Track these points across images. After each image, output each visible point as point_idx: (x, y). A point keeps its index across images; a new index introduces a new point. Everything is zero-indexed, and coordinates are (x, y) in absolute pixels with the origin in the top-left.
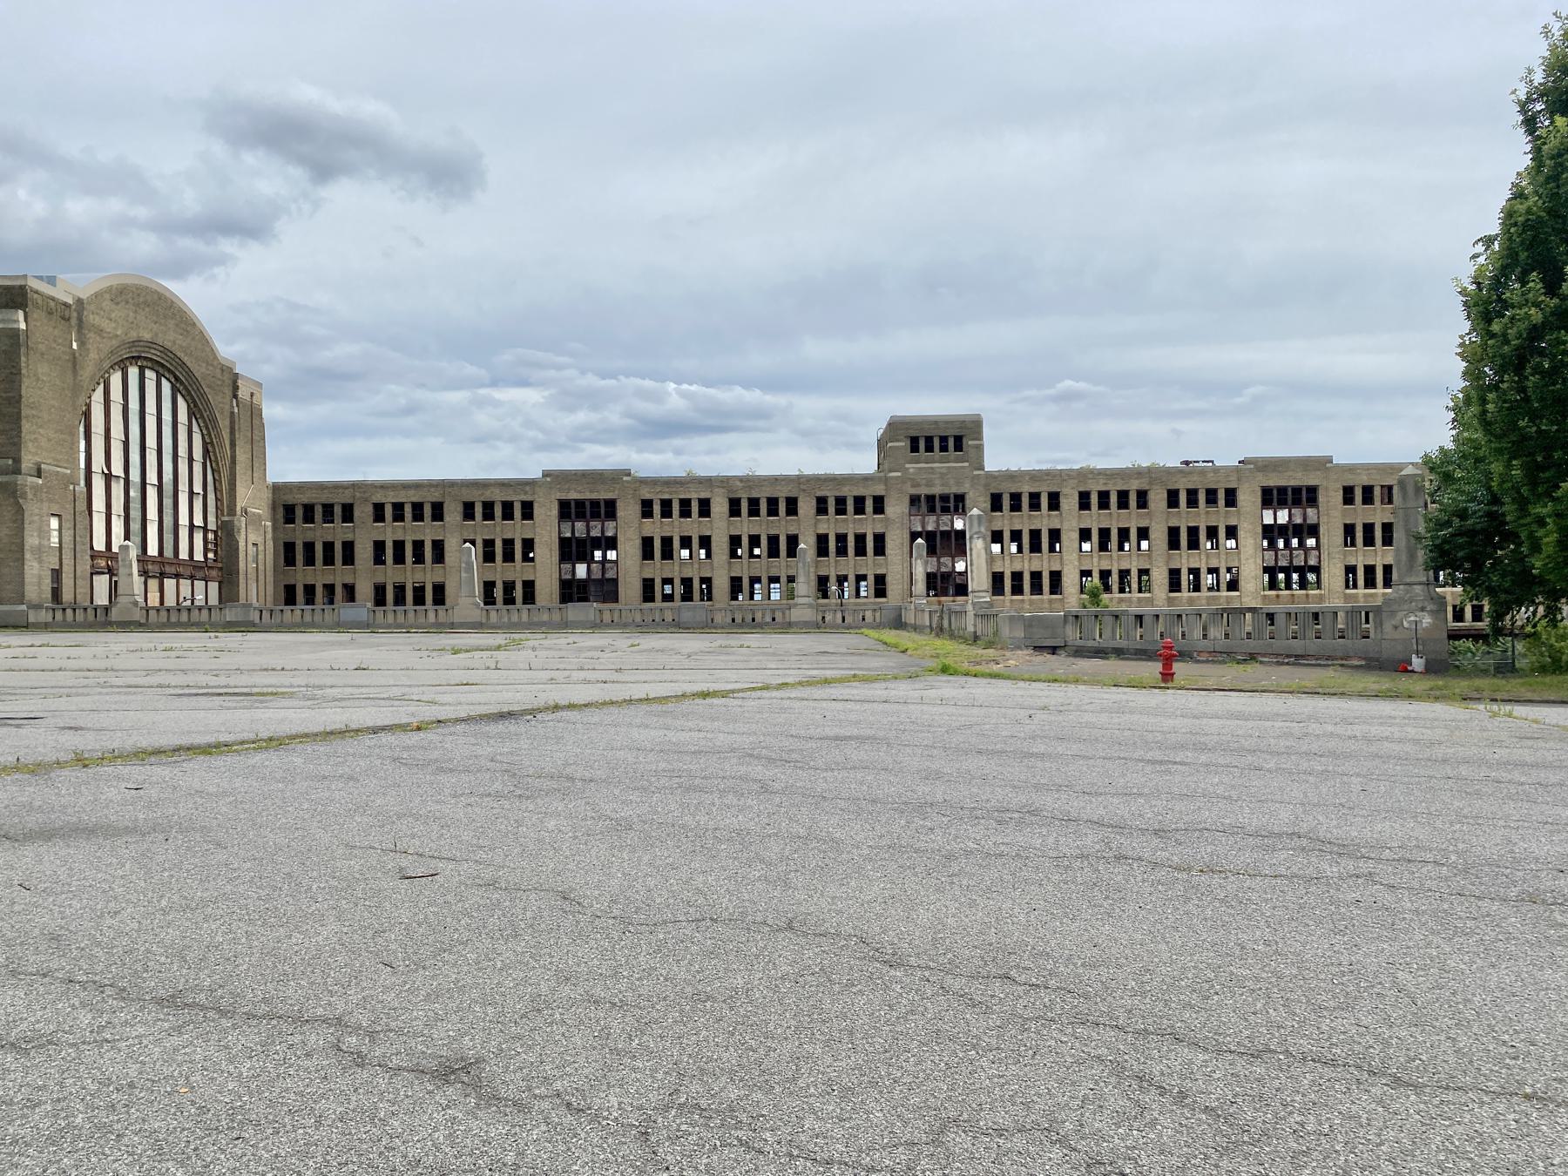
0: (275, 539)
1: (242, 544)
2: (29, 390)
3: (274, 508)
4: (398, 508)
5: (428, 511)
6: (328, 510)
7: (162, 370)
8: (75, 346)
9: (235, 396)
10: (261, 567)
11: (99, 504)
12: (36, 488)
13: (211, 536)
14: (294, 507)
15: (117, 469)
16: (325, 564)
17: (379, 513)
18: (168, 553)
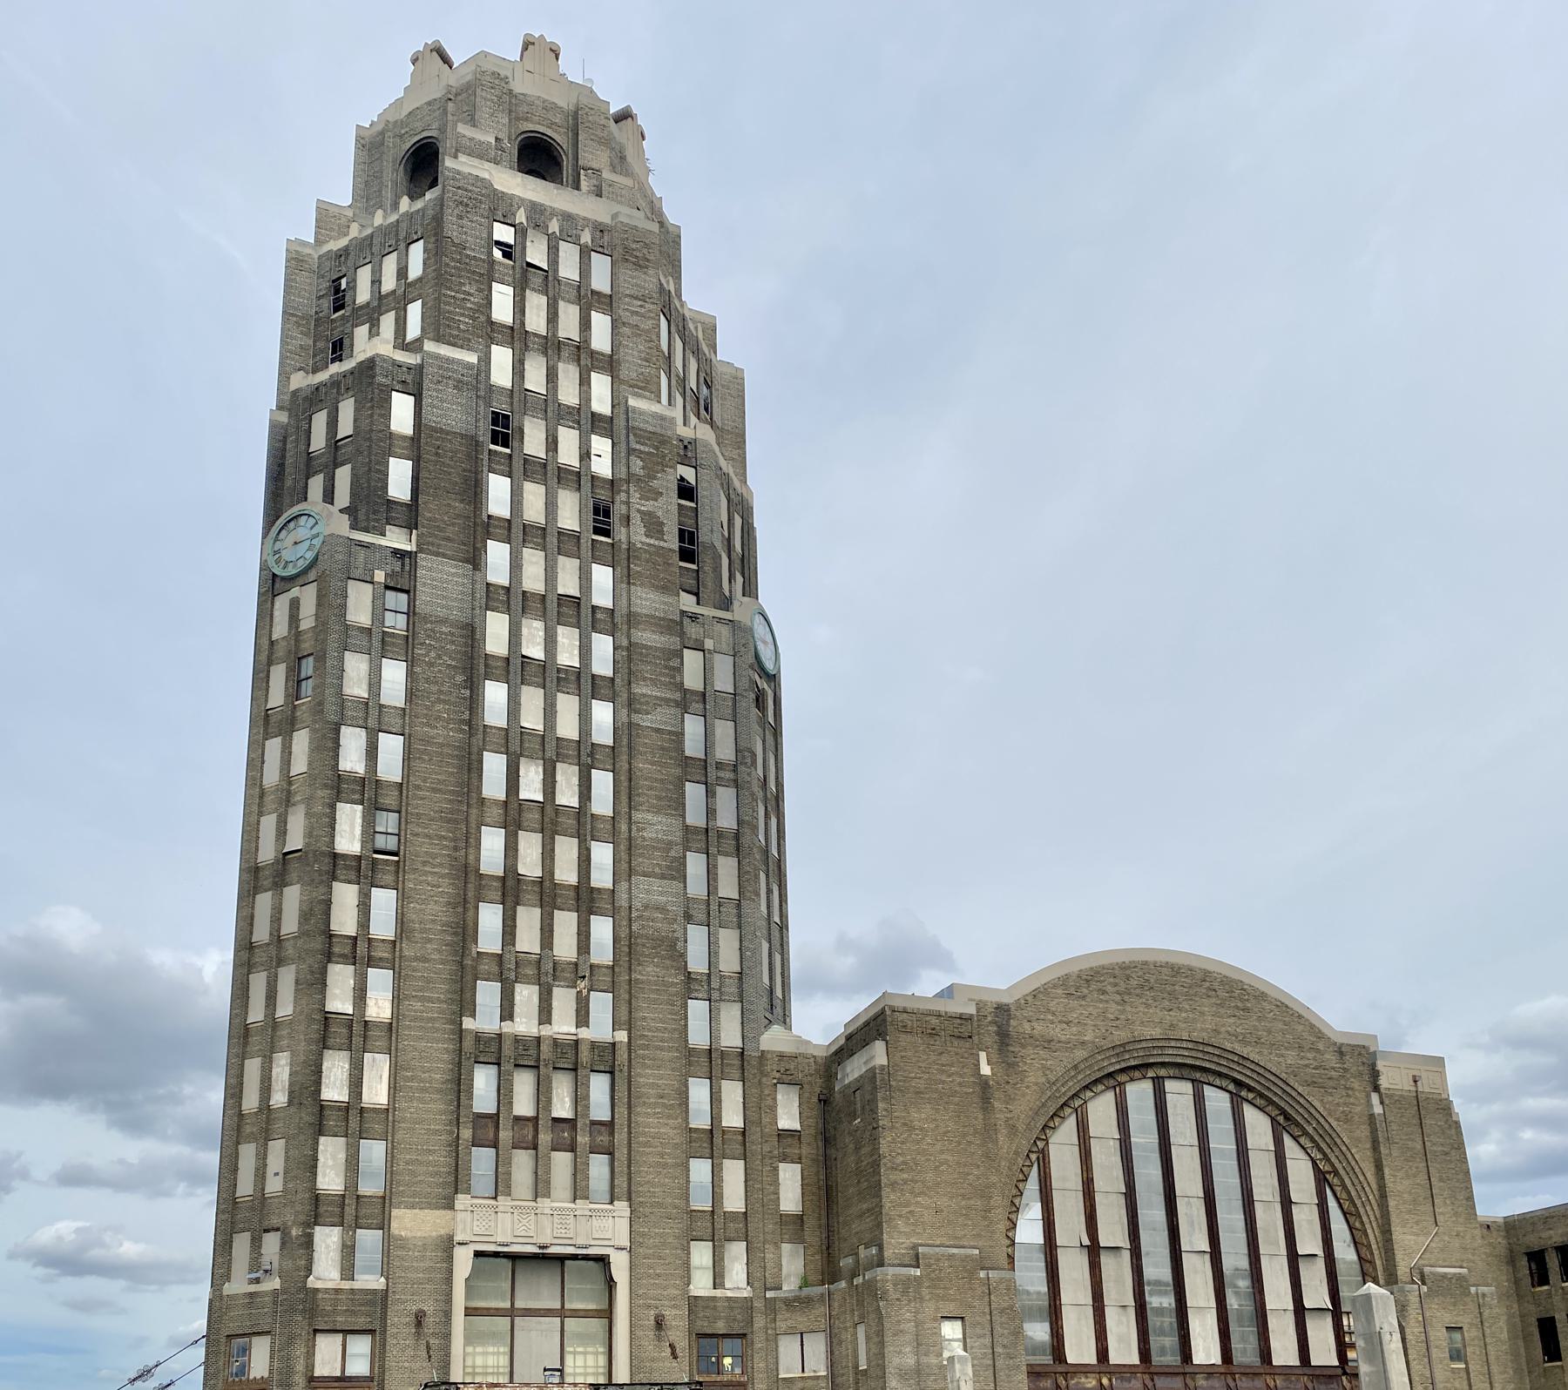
7: (1183, 1070)
8: (986, 1070)
12: (906, 1284)
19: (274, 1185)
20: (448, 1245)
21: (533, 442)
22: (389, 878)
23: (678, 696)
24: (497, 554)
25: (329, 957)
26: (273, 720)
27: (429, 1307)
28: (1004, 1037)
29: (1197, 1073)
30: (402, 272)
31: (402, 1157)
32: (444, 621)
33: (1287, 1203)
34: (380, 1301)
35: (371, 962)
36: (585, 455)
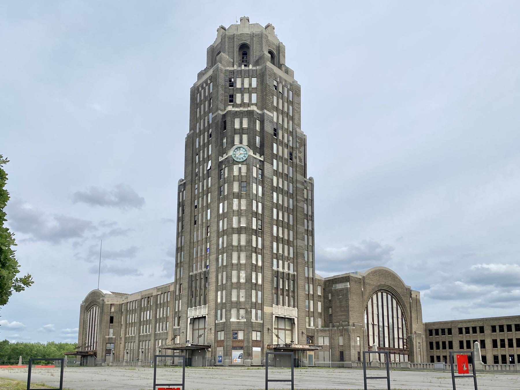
0: (427, 341)
1: (414, 343)
2: (350, 303)
3: (426, 331)
4: (467, 329)
5: (478, 330)
6: (443, 331)
9: (411, 297)
10: (422, 350)
11: (371, 333)
13: (405, 341)
14: (433, 331)
15: (376, 322)
16: (443, 349)
17: (460, 331)
18: (392, 346)
19: (242, 299)
20: (272, 314)
21: (280, 137)
22: (260, 235)
23: (303, 200)
24: (275, 161)
25: (252, 251)
26: (235, 194)
27: (270, 327)
28: (364, 282)
29: (387, 292)
30: (250, 85)
31: (265, 295)
32: (268, 178)
33: (398, 318)
34: (262, 325)
35: (259, 253)
36: (288, 141)
